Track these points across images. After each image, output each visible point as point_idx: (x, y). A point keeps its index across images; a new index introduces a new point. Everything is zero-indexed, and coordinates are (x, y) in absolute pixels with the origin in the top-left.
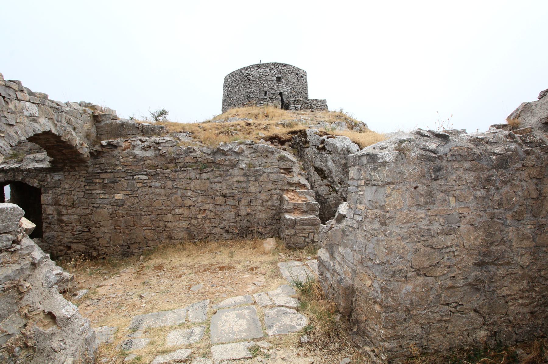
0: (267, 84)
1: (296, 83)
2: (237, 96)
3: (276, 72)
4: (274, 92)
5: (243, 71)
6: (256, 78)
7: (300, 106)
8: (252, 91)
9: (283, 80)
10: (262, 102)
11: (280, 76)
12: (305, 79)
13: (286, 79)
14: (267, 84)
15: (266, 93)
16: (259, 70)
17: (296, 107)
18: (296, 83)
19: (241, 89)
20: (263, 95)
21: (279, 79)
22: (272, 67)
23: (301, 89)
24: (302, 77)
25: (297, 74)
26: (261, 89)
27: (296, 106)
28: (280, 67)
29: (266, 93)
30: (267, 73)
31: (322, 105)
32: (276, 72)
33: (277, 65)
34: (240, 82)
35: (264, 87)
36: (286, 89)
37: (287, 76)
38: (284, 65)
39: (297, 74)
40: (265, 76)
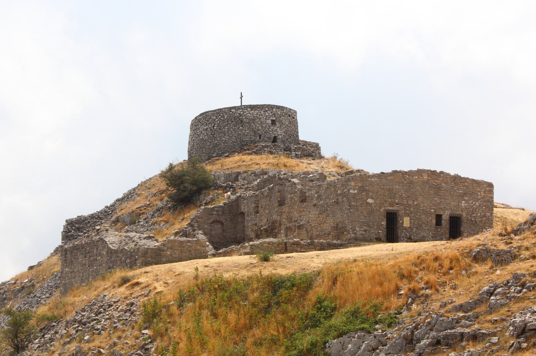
0: (262, 127)
1: (289, 125)
2: (226, 137)
3: (271, 114)
4: (269, 136)
5: (233, 110)
6: (250, 120)
7: (300, 153)
8: (246, 134)
9: (277, 123)
10: (266, 149)
11: (274, 119)
12: (296, 119)
13: (281, 122)
14: (262, 127)
15: (260, 136)
16: (253, 111)
17: (296, 155)
18: (289, 125)
19: (232, 130)
20: (258, 138)
21: (273, 122)
22: (267, 109)
23: (293, 131)
24: (294, 118)
25: (289, 116)
26: (255, 132)
27: (297, 153)
28: (274, 110)
29: (260, 136)
30: (262, 115)
31: (311, 151)
32: (271, 114)
33: (271, 107)
34: (230, 122)
35: (258, 130)
36: (280, 132)
37: (281, 119)
38: (278, 107)
39: (289, 116)
40: (260, 118)
